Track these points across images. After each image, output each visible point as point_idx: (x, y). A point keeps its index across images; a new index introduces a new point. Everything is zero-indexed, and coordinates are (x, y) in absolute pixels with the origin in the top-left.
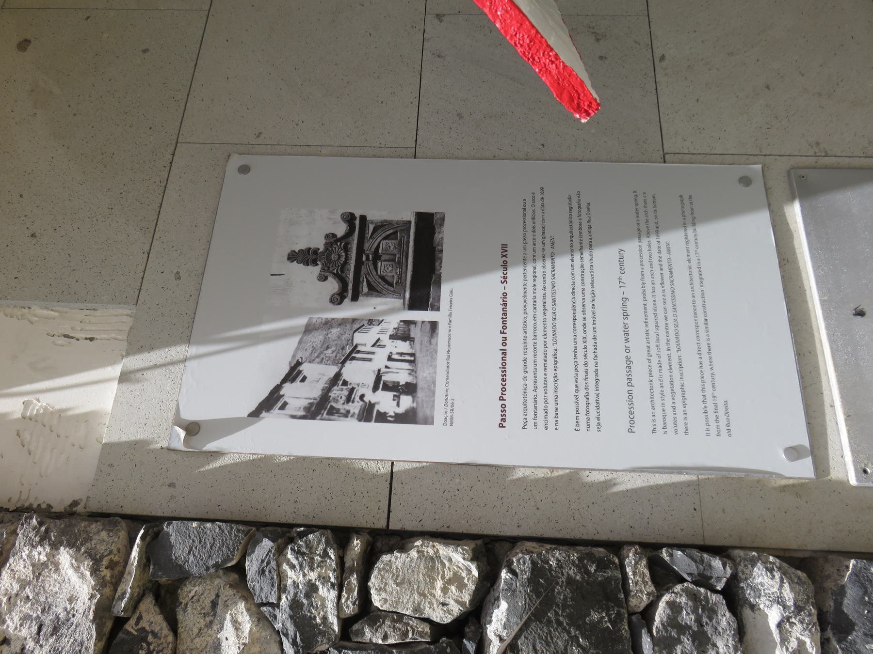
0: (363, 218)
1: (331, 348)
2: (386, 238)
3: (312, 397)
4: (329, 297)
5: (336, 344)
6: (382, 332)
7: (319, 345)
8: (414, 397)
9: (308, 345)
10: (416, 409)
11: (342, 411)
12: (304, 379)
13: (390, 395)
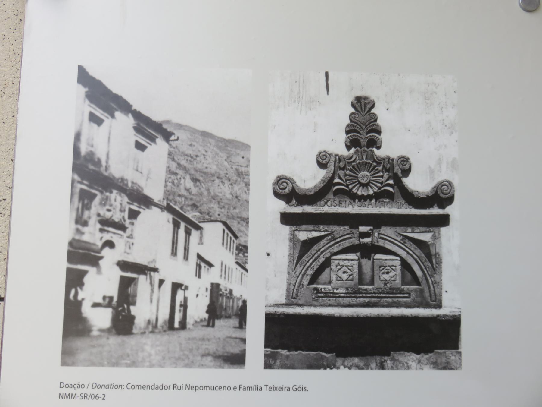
0: (444, 220)
1: (195, 186)
2: (405, 265)
3: (110, 163)
4: (288, 174)
5: (201, 194)
6: (224, 269)
7: (199, 166)
8: (109, 331)
9: (201, 148)
10: (89, 336)
11: (86, 213)
12: (140, 147)
13: (113, 291)
